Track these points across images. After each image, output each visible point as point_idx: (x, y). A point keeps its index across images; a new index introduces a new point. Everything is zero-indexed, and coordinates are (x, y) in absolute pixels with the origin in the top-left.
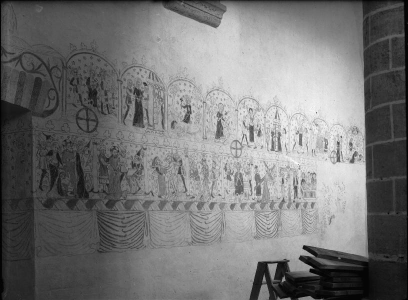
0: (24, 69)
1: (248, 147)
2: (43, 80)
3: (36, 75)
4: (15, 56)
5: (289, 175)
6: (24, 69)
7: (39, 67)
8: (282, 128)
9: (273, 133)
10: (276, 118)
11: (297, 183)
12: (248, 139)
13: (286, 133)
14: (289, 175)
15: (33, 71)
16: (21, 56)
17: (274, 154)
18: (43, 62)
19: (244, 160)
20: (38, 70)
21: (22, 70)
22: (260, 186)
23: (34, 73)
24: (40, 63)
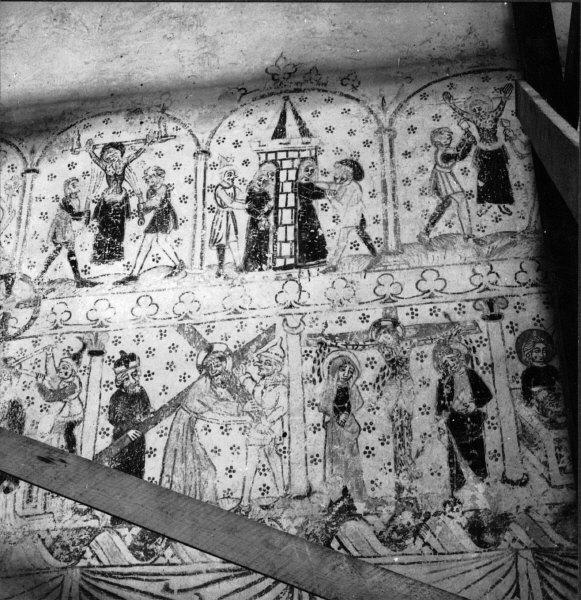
1: (82, 283)
5: (396, 366)
8: (326, 161)
9: (257, 201)
10: (280, 132)
11: (482, 394)
12: (84, 257)
13: (358, 174)
14: (396, 366)
17: (262, 286)
19: (46, 341)
22: (140, 442)
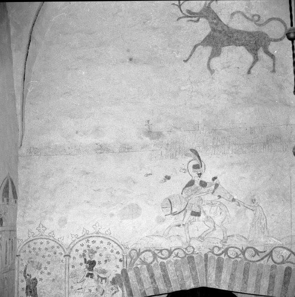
0: (275, 263)
2: (293, 268)
3: (285, 266)
4: (266, 253)
6: (275, 263)
7: (289, 257)
15: (283, 262)
16: (271, 251)
18: (292, 252)
20: (288, 260)
21: (273, 263)
23: (284, 263)
24: (288, 253)
